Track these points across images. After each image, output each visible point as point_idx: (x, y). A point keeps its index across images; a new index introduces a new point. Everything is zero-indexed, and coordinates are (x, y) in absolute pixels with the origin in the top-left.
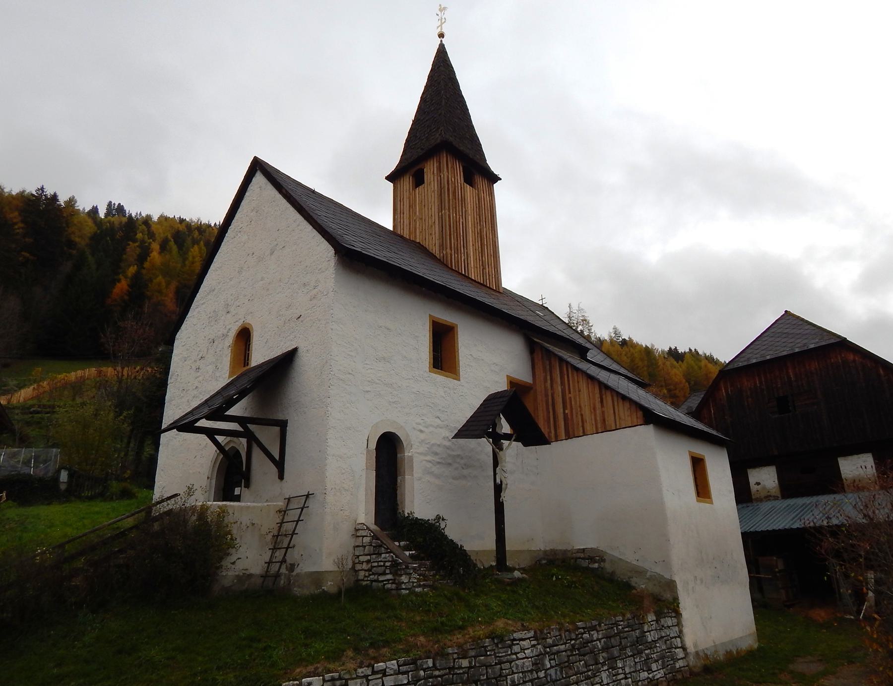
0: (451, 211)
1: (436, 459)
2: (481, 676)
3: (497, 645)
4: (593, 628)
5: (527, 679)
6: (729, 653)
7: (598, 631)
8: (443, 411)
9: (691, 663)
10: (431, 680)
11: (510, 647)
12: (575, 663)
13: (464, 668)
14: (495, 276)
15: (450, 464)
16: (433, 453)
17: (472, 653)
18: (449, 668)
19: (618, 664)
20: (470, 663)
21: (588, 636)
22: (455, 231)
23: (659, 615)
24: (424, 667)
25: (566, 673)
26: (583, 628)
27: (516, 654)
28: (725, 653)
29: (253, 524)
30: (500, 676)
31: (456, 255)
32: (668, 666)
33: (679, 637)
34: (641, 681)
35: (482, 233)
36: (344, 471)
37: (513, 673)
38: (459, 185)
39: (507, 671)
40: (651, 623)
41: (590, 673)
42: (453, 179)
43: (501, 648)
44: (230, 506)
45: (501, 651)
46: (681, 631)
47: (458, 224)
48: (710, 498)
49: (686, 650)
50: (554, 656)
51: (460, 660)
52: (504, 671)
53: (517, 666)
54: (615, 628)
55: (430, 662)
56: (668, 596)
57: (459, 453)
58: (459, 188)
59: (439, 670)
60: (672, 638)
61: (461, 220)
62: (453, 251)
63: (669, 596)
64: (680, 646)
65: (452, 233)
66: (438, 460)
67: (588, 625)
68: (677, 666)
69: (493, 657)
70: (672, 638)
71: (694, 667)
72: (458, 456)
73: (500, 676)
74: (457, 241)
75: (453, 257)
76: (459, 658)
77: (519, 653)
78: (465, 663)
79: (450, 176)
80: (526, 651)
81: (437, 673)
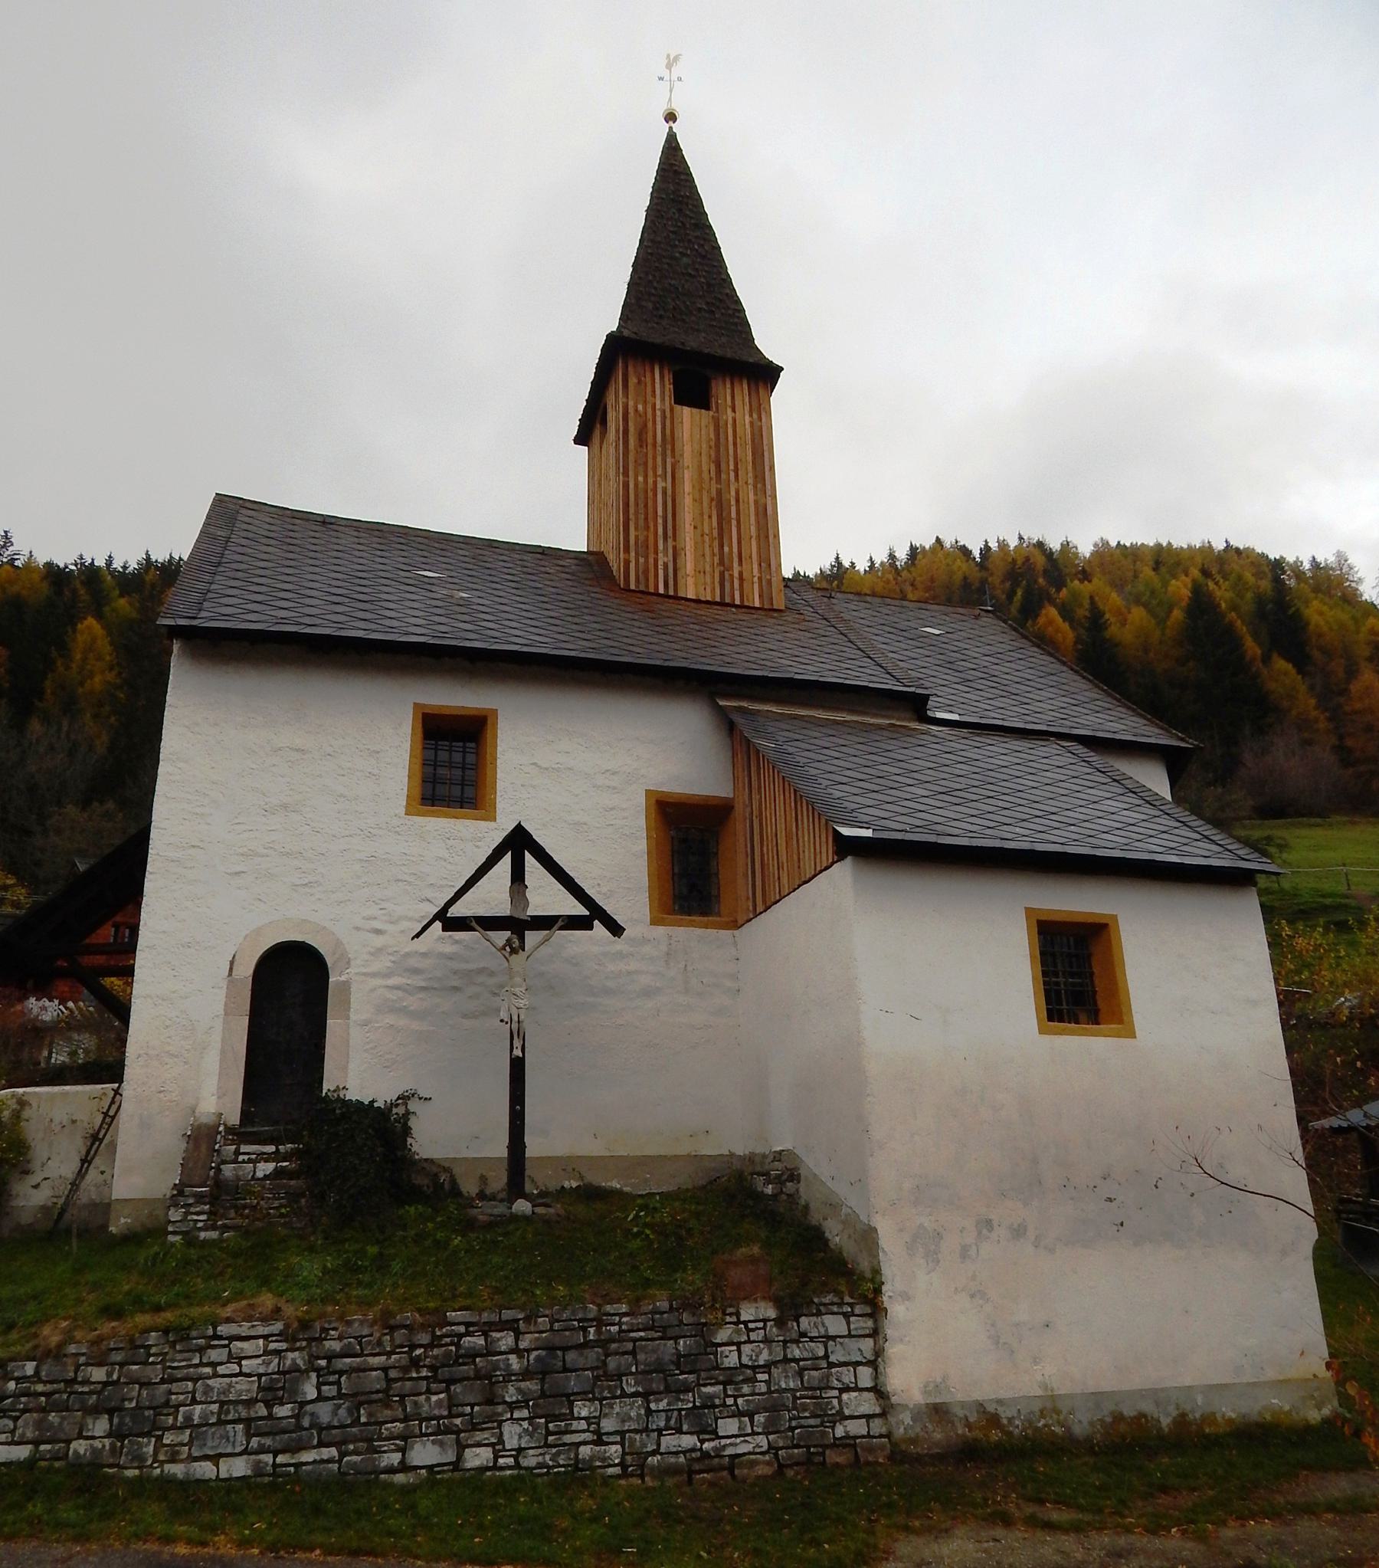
0: (631, 473)
1: (418, 981)
2: (126, 1403)
3: (173, 1344)
4: (511, 1326)
5: (230, 1417)
6: (1181, 1421)
7: (518, 1334)
8: (442, 886)
9: (902, 1430)
10: (23, 1399)
11: (201, 1350)
12: (409, 1396)
13: (94, 1383)
14: (760, 579)
15: (456, 989)
16: (407, 970)
17: (118, 1357)
18: (66, 1382)
19: (576, 1410)
20: (109, 1374)
21: (483, 1342)
22: (642, 511)
23: (791, 1308)
24: (16, 1374)
25: (370, 1415)
26: (467, 1324)
27: (214, 1365)
28: (1109, 1420)
29: (74, 1122)
30: (167, 1404)
31: (642, 560)
32: (792, 1429)
33: (873, 1364)
34: (661, 1454)
35: (725, 496)
36: (168, 1023)
37: (194, 1402)
38: (658, 413)
39: (182, 1397)
40: (751, 1326)
41: (458, 1421)
42: (640, 407)
43: (181, 1352)
44: (35, 1093)
45: (179, 1356)
46: (879, 1353)
47: (650, 494)
48: (1121, 1021)
49: (888, 1398)
50: (340, 1377)
51: (90, 1369)
52: (173, 1397)
53: (208, 1389)
54: (592, 1330)
55: (30, 1368)
56: (864, 1265)
57: (481, 965)
58: (658, 419)
59: (45, 1383)
60: (831, 1365)
61: (660, 485)
62: (633, 554)
63: (866, 1264)
64: (869, 1384)
65: (632, 516)
66: (423, 984)
67: (486, 1317)
68: (840, 1431)
69: (159, 1366)
70: (831, 1365)
71: (914, 1441)
72: (481, 971)
73: (167, 1404)
74: (647, 528)
75: (632, 565)
76: (87, 1364)
77: (221, 1364)
78: (98, 1374)
79: (631, 403)
80: (243, 1362)
81: (40, 1388)
